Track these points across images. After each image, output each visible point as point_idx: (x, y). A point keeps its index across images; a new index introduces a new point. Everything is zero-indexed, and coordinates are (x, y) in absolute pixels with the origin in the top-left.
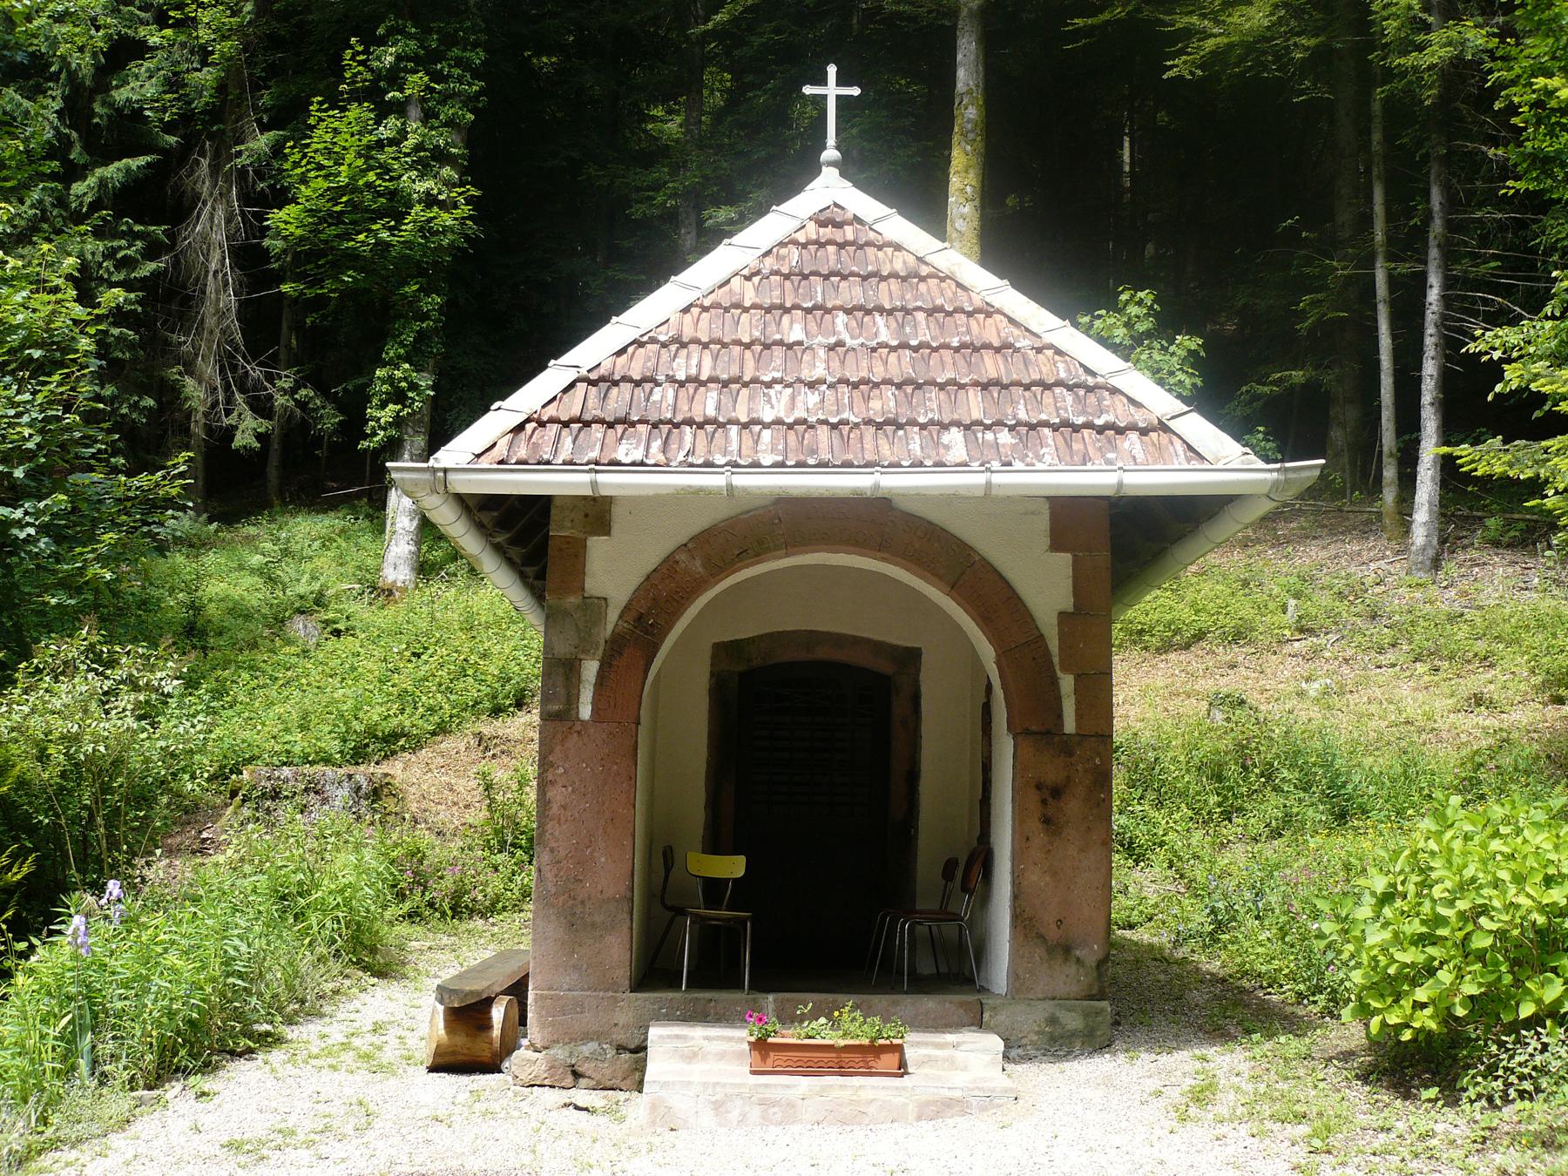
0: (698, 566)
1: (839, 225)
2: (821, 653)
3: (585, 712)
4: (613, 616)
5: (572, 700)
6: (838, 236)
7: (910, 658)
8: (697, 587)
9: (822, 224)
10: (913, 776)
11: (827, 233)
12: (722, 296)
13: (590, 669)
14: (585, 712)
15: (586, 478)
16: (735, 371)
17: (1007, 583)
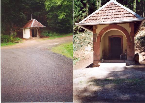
0: (103, 31)
1: (112, 3)
2: (116, 36)
3: (96, 41)
4: (98, 34)
5: (95, 40)
6: (112, 4)
7: (123, 36)
8: (104, 32)
9: (111, 3)
10: (123, 45)
11: (111, 4)
12: (102, 10)
13: (96, 38)
14: (96, 41)
15: (89, 24)
16: (102, 15)
17: (126, 30)
